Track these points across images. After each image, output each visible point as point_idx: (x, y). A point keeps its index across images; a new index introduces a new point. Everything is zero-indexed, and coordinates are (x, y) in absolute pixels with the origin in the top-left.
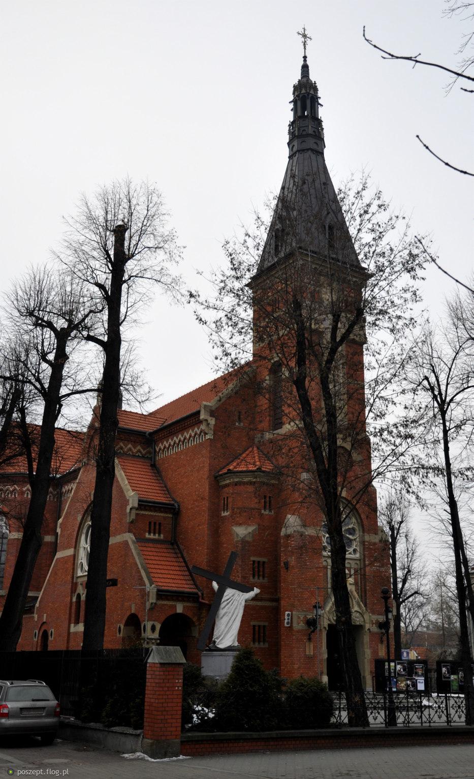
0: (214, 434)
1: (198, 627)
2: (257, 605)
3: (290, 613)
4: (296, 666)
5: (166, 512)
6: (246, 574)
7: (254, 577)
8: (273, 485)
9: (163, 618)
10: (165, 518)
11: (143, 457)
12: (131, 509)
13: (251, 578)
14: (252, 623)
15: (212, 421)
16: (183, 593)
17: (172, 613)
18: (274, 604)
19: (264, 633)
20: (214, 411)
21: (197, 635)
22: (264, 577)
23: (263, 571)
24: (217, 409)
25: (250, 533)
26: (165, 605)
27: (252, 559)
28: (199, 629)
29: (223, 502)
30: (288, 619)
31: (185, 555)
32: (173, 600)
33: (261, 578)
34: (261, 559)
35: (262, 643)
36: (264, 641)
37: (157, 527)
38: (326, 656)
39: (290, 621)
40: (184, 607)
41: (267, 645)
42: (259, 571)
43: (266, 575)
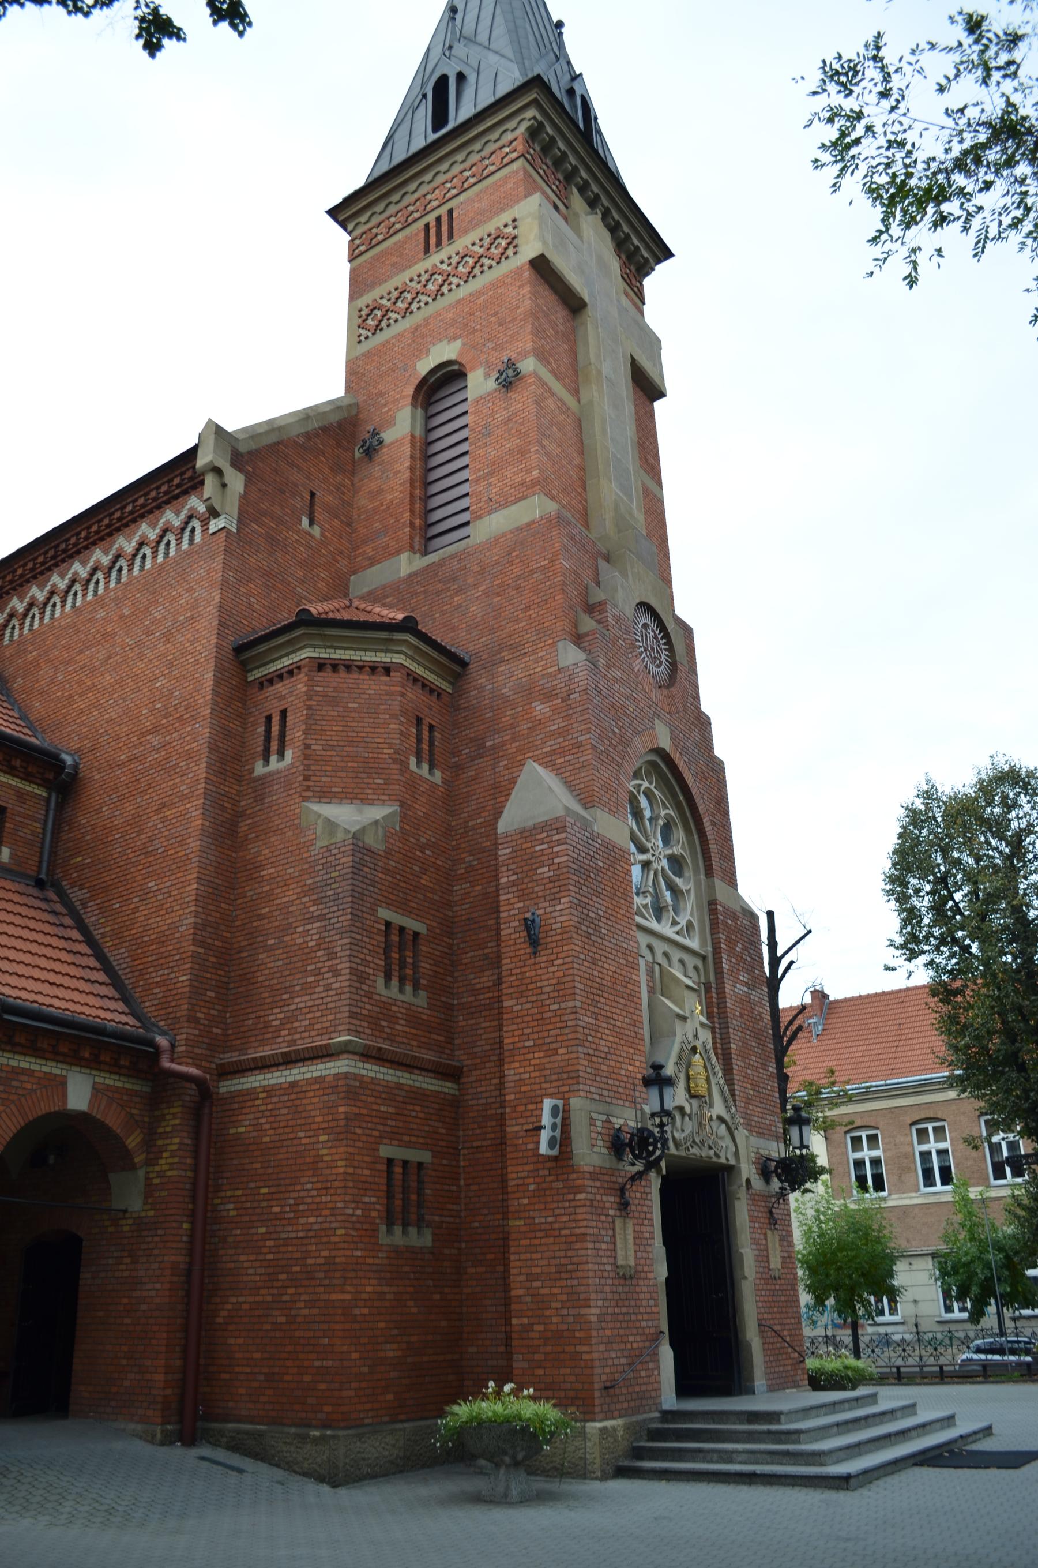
0: (242, 520)
1: (141, 1173)
2: (399, 1086)
3: (560, 1103)
4: (593, 1313)
5: (28, 777)
6: (365, 963)
7: (388, 978)
8: (439, 695)
10: (20, 795)
13: (380, 981)
14: (386, 1151)
15: (236, 482)
16: (98, 1030)
17: (43, 1109)
18: (448, 1087)
19: (420, 1193)
20: (242, 455)
21: (136, 1204)
22: (416, 987)
23: (415, 967)
24: (250, 453)
25: (376, 822)
27: (384, 913)
28: (147, 1179)
29: (261, 730)
30: (554, 1127)
31: (90, 920)
32: (55, 1055)
33: (409, 989)
34: (412, 924)
35: (413, 1230)
36: (420, 1223)
38: (662, 1271)
39: (557, 1134)
40: (96, 1090)
41: (427, 1240)
42: (402, 964)
43: (423, 982)
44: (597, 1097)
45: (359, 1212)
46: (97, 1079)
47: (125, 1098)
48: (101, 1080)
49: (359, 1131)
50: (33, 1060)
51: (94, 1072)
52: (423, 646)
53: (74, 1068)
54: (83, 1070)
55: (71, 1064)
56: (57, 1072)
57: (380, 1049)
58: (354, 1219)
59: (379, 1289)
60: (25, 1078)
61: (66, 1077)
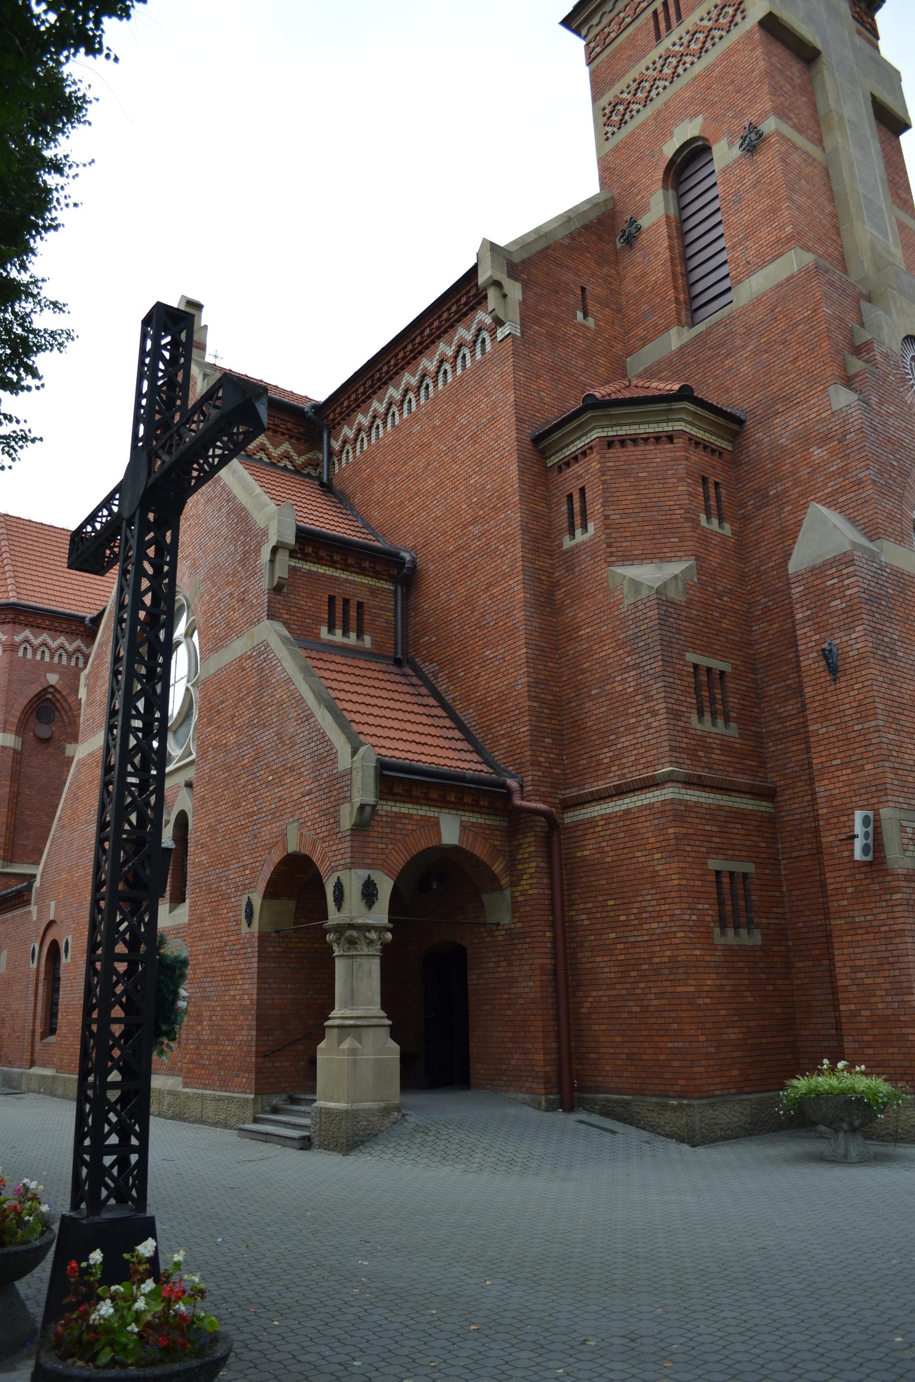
0: (524, 325)
1: (507, 893)
2: (720, 808)
3: (871, 814)
5: (376, 575)
6: (679, 702)
7: (701, 714)
8: (720, 454)
9: (399, 860)
10: (373, 591)
11: (297, 471)
12: (275, 550)
13: (694, 717)
14: (714, 864)
15: (514, 290)
16: (460, 778)
17: (424, 844)
18: (764, 806)
19: (747, 899)
20: (516, 265)
21: (505, 918)
22: (727, 720)
23: (724, 702)
24: (523, 262)
25: (676, 577)
26: (405, 816)
27: (691, 657)
28: (513, 897)
29: (564, 508)
30: (866, 836)
31: (441, 688)
32: (427, 801)
33: (720, 722)
34: (718, 665)
35: (743, 932)
36: (750, 925)
37: (353, 613)
39: (870, 841)
40: (464, 827)
41: (756, 939)
42: (713, 700)
43: (733, 715)
44: (905, 806)
45: (694, 918)
46: (463, 818)
47: (488, 832)
48: (466, 819)
49: (688, 848)
50: (410, 806)
51: (460, 813)
52: (700, 411)
53: (443, 810)
54: (451, 812)
55: (441, 807)
56: (431, 814)
57: (700, 776)
58: (691, 923)
59: (718, 982)
60: (406, 821)
61: (438, 818)
